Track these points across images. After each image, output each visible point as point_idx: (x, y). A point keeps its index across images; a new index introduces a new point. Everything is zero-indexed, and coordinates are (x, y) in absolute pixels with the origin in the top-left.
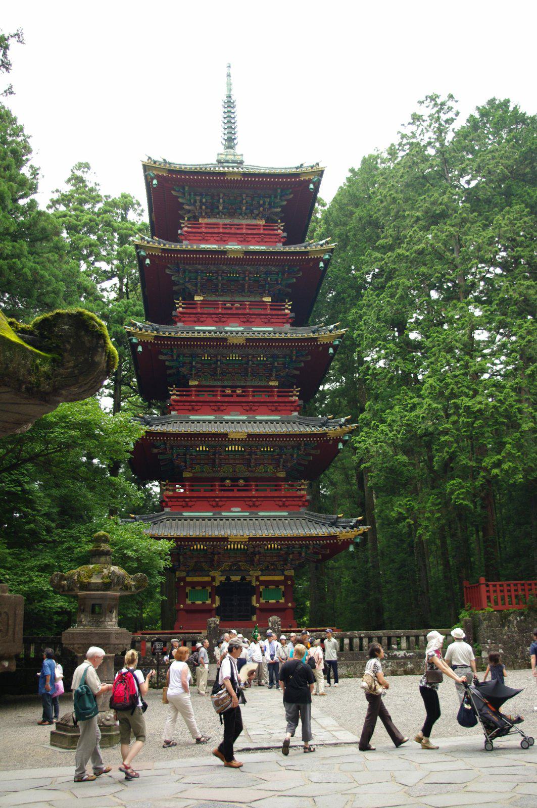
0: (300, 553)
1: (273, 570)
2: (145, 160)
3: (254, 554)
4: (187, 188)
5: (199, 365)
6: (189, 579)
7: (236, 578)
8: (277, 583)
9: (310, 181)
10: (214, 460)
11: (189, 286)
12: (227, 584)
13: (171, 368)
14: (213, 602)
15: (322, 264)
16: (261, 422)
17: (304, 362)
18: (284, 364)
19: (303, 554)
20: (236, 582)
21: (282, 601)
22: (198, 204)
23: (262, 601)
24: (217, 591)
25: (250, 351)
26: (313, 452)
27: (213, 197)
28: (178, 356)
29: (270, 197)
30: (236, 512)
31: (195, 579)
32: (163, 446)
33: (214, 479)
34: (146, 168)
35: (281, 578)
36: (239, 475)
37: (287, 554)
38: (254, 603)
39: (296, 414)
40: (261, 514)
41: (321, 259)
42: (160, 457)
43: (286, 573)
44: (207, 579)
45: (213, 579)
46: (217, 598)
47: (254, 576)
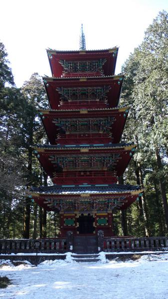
0: (114, 203)
1: (103, 210)
2: (48, 49)
3: (93, 203)
4: (65, 61)
5: (70, 126)
6: (65, 215)
7: (86, 214)
8: (104, 217)
9: (113, 53)
10: (76, 164)
11: (66, 96)
12: (82, 217)
13: (57, 127)
14: (76, 225)
15: (119, 82)
16: (96, 147)
17: (114, 122)
18: (105, 123)
19: (116, 203)
20: (86, 216)
21: (107, 224)
22: (69, 67)
23: (98, 224)
24: (77, 220)
25: (91, 119)
26: (118, 158)
27: (75, 64)
28: (61, 122)
29: (97, 63)
30: (85, 185)
31: (68, 215)
32: (53, 158)
33: (76, 172)
34: (48, 51)
35: (107, 214)
36: (87, 170)
37: (108, 203)
38: (94, 225)
39: (111, 143)
40: (96, 185)
41: (118, 80)
42: (52, 162)
43: (108, 212)
44: (74, 215)
45: (76, 215)
46: (78, 224)
47: (94, 213)
